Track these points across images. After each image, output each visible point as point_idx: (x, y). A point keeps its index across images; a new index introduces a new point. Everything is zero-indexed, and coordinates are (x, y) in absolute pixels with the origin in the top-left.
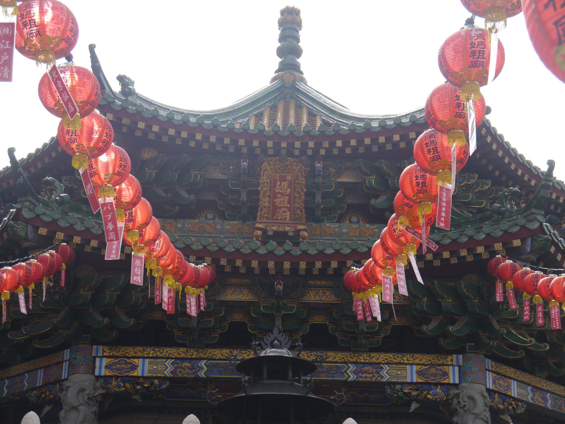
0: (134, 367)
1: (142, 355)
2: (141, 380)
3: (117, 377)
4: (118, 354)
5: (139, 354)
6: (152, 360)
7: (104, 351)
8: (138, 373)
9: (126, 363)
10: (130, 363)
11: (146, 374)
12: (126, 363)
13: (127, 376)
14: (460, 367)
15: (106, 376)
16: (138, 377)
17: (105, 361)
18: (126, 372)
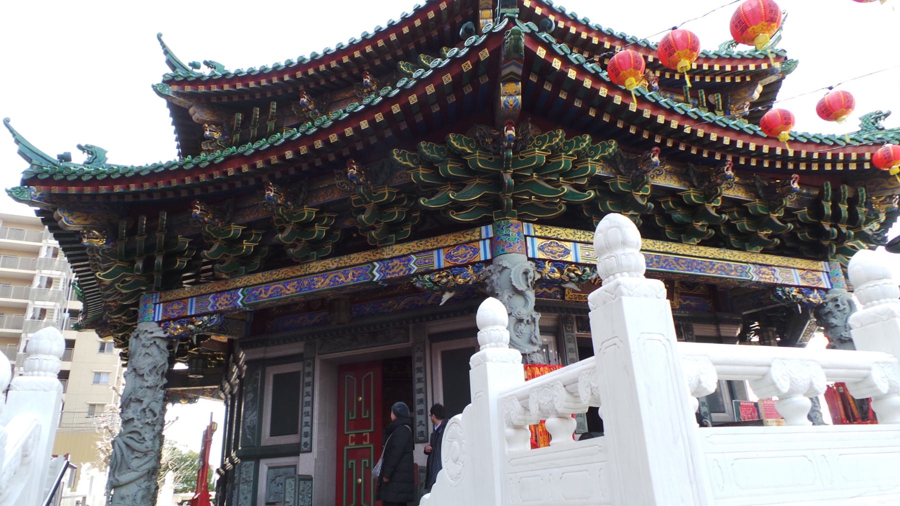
0: (567, 252)
1: (574, 239)
2: (573, 267)
3: (550, 261)
4: (550, 235)
5: (571, 238)
6: (583, 245)
7: (535, 231)
8: (570, 258)
9: (558, 246)
10: (563, 247)
11: (581, 261)
12: (558, 246)
13: (560, 261)
14: (827, 273)
15: (539, 259)
16: (571, 263)
17: (538, 242)
18: (559, 256)
